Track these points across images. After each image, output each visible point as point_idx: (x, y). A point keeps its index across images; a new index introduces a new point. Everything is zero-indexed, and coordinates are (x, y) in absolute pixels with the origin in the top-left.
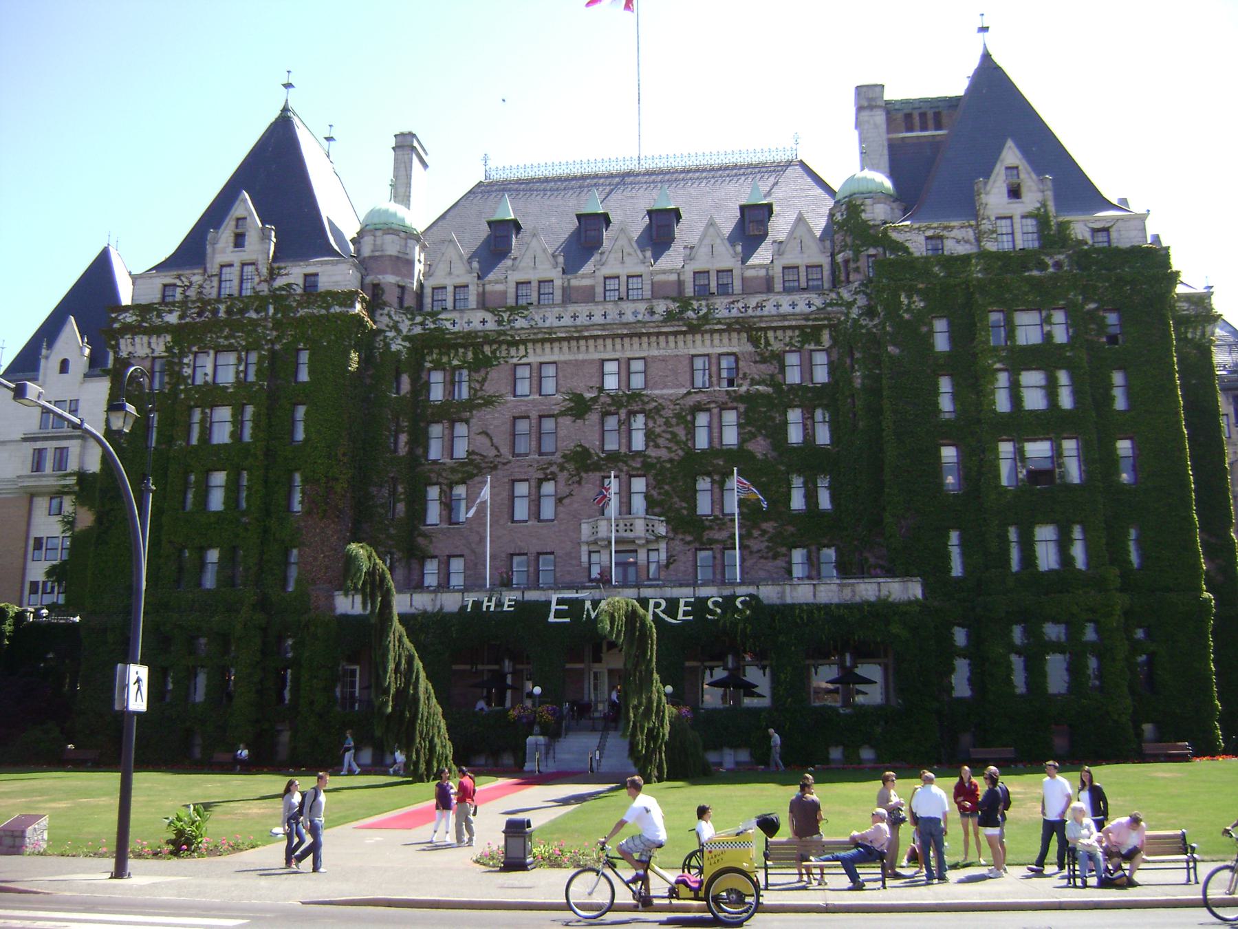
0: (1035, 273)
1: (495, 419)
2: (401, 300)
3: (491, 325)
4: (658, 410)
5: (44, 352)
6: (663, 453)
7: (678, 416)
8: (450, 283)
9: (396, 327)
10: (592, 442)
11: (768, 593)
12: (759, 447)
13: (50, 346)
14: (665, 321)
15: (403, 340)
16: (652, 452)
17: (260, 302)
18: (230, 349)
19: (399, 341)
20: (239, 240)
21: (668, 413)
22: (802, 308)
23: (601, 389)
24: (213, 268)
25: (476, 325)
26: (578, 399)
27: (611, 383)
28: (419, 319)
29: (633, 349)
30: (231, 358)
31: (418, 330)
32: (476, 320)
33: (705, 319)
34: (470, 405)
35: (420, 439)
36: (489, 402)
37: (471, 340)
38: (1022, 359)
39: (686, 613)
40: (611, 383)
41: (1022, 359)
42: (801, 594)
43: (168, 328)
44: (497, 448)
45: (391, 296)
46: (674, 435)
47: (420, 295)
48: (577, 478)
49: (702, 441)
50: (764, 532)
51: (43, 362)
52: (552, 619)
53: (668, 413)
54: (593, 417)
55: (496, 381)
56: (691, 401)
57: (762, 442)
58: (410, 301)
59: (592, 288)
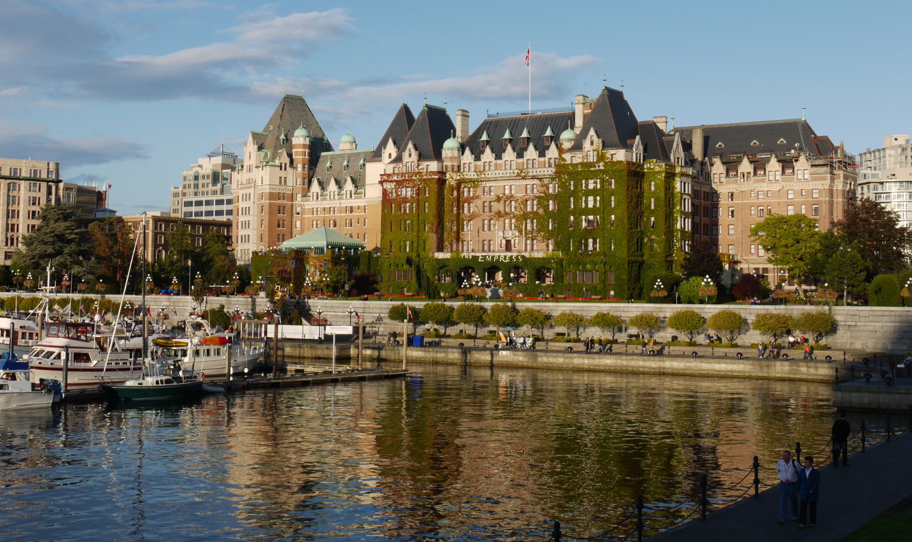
0: (593, 169)
1: (479, 202)
2: (453, 169)
3: (476, 177)
4: (517, 200)
6: (518, 213)
8: (467, 162)
9: (452, 178)
10: (502, 209)
11: (527, 255)
12: (541, 211)
13: (385, 148)
14: (517, 176)
16: (516, 212)
17: (416, 174)
18: (409, 187)
20: (410, 155)
22: (550, 173)
23: (504, 194)
24: (404, 164)
25: (472, 177)
26: (498, 197)
27: (507, 192)
29: (511, 183)
30: (409, 189)
31: (458, 178)
32: (472, 175)
33: (525, 176)
34: (473, 198)
35: (460, 207)
36: (477, 197)
37: (471, 181)
38: (588, 193)
40: (507, 192)
41: (588, 193)
42: (536, 255)
43: (395, 181)
45: (450, 169)
47: (459, 167)
49: (529, 209)
54: (502, 202)
55: (479, 192)
56: (525, 198)
58: (456, 169)
59: (501, 164)
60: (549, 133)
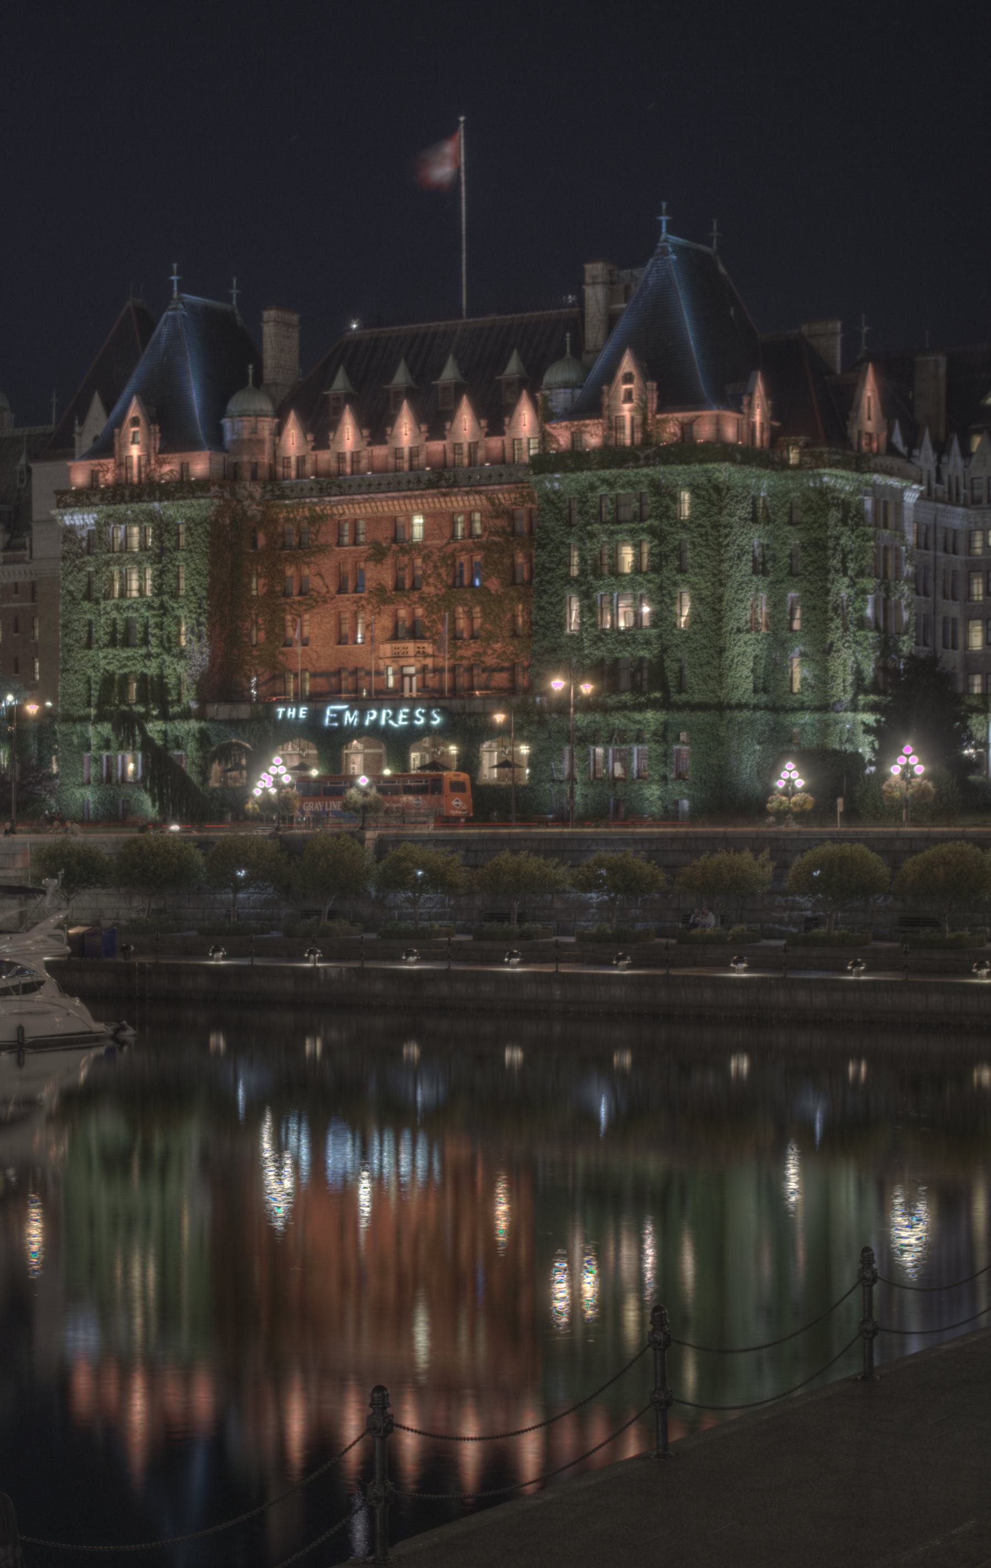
5: (77, 429)
7: (443, 559)
9: (251, 497)
13: (82, 423)
15: (258, 505)
19: (254, 507)
21: (435, 557)
28: (269, 487)
39: (404, 720)
44: (327, 587)
46: (439, 575)
48: (377, 610)
50: (495, 651)
51: (77, 437)
52: (327, 721)
53: (435, 557)
57: (496, 582)
60: (513, 367)
